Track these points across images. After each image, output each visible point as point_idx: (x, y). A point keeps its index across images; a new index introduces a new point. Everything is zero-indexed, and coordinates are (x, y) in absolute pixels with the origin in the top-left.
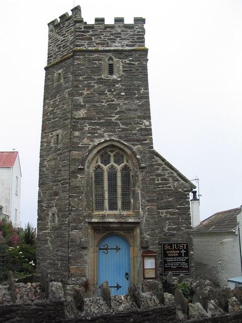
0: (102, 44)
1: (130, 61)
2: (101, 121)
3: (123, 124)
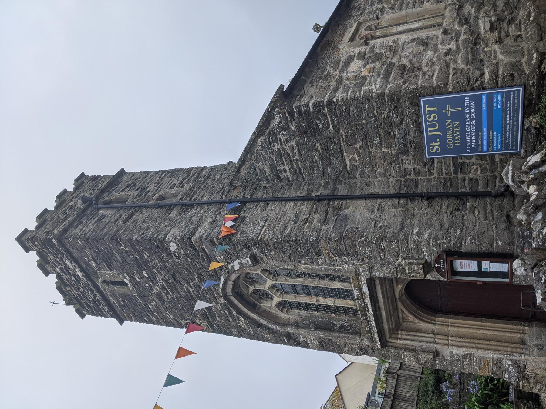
3: (192, 280)
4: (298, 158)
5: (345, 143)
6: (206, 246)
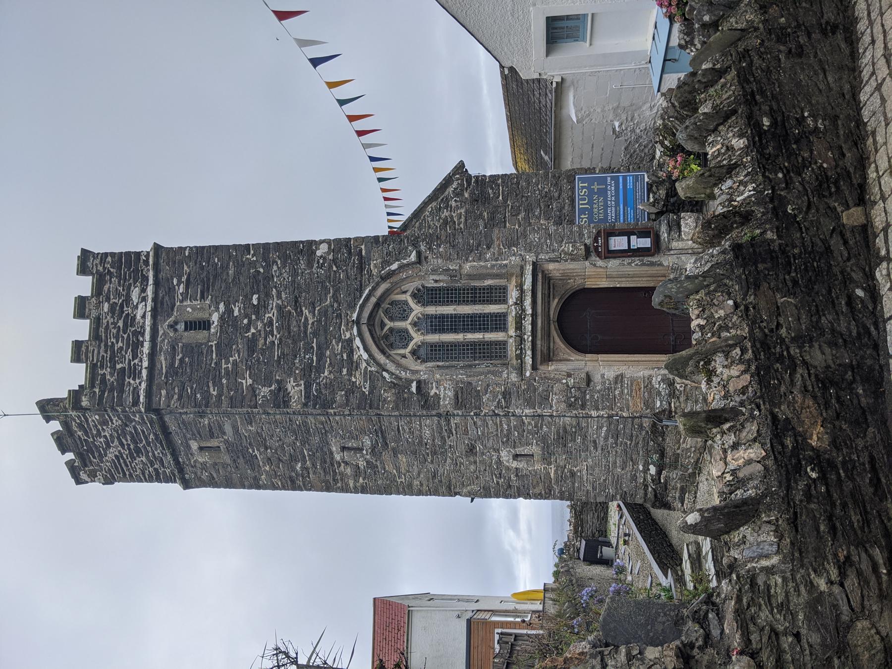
0: (136, 346)
2: (314, 345)
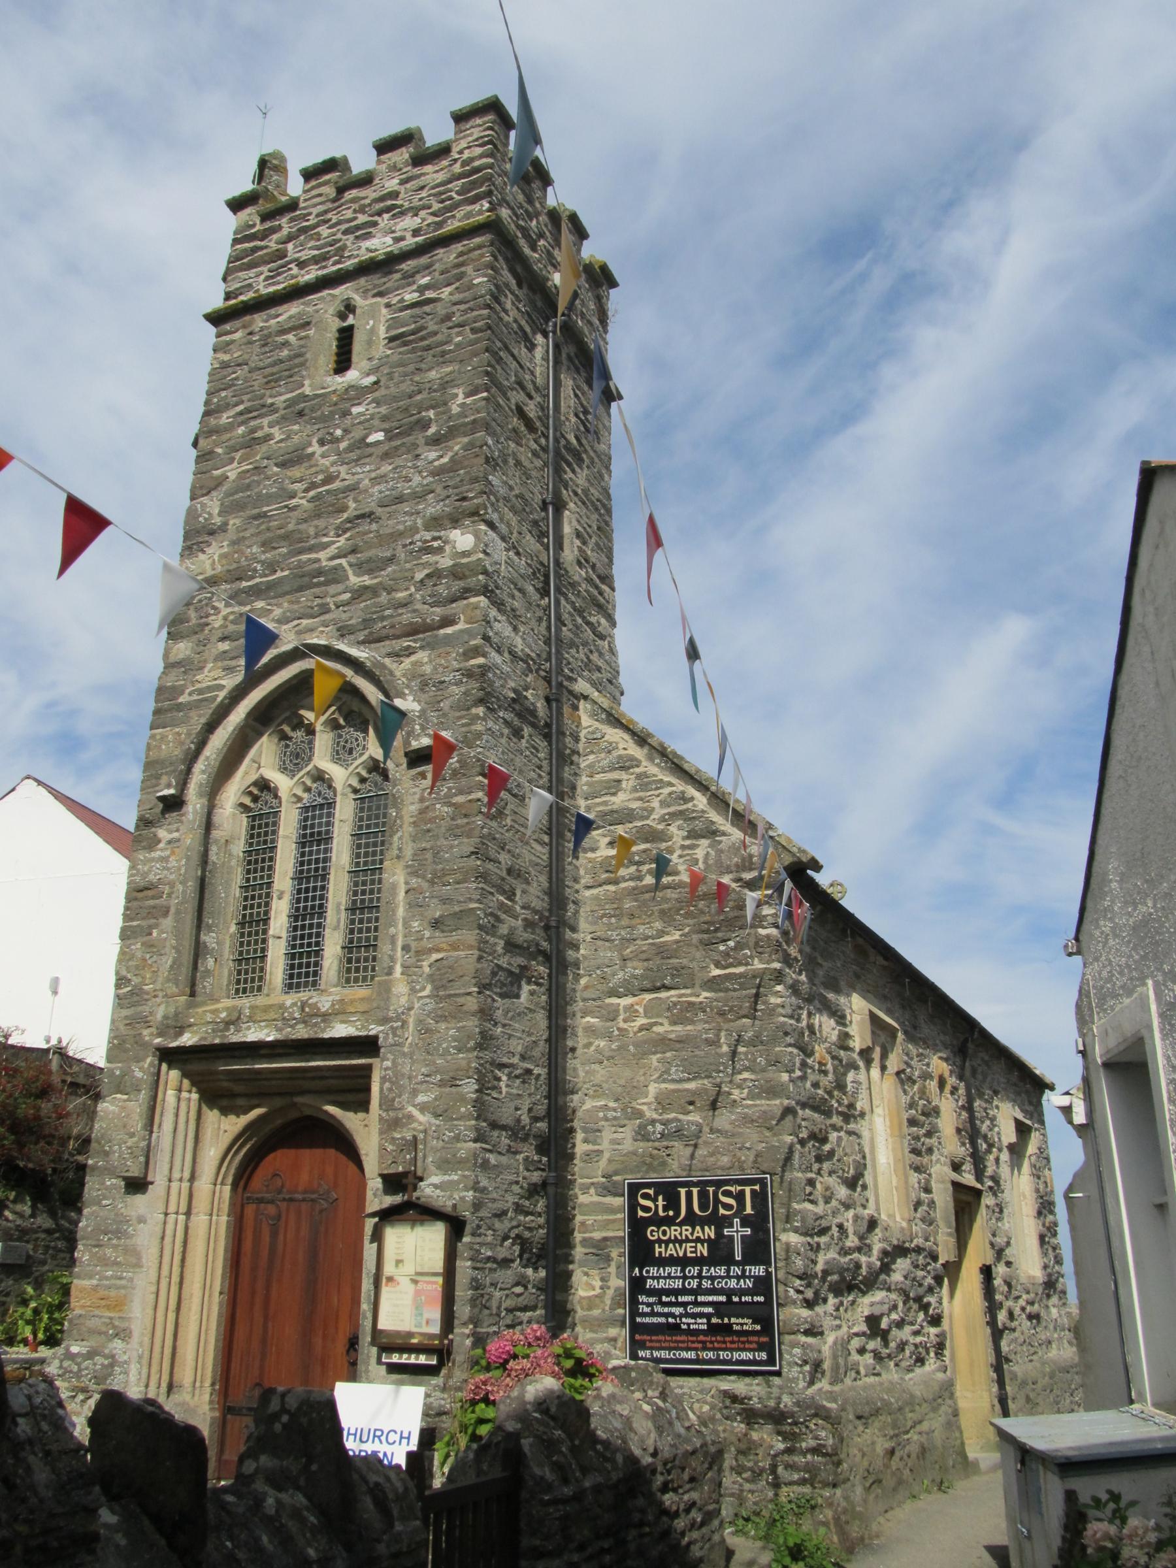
1: (422, 289)
2: (279, 574)
3: (360, 568)
4: (644, 883)
5: (674, 999)
6: (462, 631)
